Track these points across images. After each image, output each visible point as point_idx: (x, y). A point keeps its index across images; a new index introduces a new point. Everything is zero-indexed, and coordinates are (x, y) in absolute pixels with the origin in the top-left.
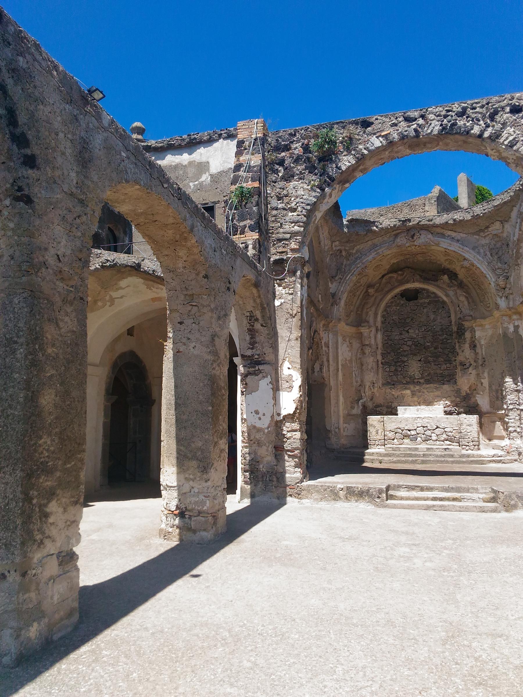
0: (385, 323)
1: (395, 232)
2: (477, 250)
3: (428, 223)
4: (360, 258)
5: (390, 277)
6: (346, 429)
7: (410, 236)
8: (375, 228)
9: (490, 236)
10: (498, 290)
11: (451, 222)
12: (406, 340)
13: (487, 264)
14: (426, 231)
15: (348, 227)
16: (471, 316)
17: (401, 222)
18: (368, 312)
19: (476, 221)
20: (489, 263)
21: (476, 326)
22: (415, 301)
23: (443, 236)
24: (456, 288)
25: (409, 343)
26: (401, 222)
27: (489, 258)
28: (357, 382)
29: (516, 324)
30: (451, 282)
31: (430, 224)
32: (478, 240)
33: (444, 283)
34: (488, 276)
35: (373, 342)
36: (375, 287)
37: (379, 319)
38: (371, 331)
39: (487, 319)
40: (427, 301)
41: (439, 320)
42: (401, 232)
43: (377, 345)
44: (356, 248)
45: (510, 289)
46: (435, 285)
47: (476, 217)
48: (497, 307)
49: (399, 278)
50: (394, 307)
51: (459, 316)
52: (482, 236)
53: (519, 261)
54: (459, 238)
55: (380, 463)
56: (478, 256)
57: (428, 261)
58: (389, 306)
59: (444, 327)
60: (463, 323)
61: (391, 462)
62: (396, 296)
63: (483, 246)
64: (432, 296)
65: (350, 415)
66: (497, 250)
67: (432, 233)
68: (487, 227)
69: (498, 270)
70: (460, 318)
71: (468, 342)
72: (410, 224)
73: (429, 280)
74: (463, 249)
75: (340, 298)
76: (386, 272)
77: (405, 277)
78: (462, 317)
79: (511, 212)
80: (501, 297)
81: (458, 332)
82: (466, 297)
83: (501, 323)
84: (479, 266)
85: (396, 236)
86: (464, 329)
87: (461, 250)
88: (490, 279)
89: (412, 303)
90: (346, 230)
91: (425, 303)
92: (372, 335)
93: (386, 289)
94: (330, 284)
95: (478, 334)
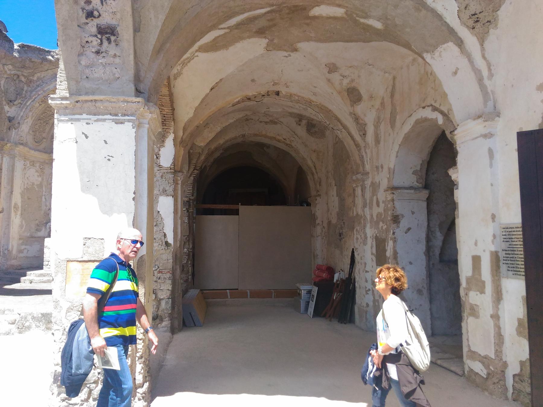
4: (42, 85)
6: (25, 251)
28: (46, 206)
55: (31, 283)
61: (40, 282)
65: (32, 237)
75: (19, 123)
90: (16, 54)
94: (6, 108)
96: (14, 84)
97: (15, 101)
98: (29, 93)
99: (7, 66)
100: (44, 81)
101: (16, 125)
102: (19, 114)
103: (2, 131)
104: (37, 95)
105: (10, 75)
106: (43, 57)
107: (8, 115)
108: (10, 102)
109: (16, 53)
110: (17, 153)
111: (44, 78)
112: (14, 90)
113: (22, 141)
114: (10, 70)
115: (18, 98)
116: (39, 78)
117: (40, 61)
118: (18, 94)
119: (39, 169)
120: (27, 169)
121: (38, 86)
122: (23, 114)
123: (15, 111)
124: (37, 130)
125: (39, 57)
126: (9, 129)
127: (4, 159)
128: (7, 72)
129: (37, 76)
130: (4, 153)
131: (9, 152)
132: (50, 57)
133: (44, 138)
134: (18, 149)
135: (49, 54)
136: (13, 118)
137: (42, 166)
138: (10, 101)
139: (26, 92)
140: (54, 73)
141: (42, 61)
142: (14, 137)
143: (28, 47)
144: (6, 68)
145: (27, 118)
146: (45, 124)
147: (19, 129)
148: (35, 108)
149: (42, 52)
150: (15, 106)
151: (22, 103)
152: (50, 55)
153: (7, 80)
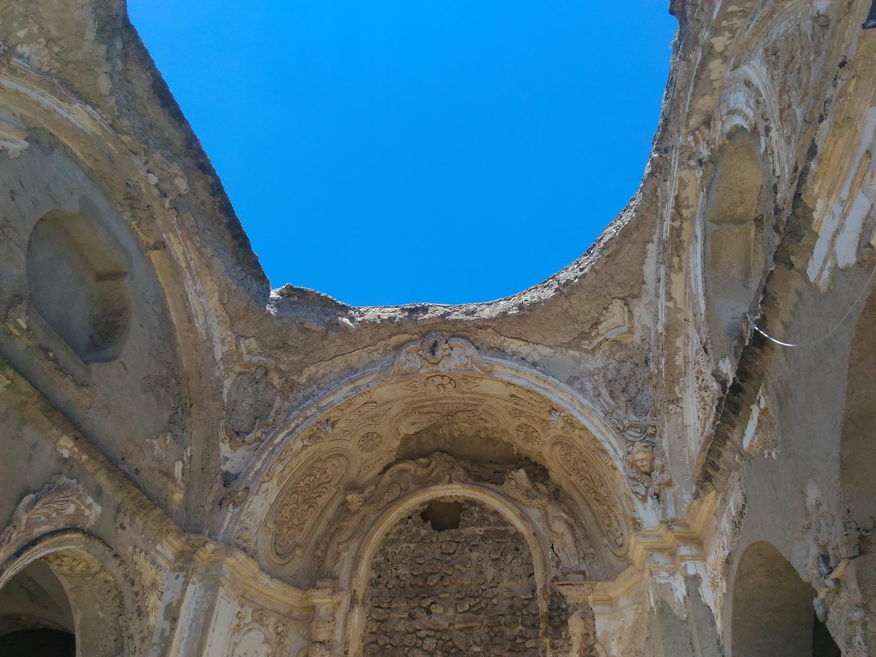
0: (377, 584)
1: (394, 340)
2: (577, 385)
3: (465, 318)
5: (402, 471)
7: (428, 349)
8: (346, 320)
9: (605, 347)
10: (634, 479)
11: (514, 311)
12: (422, 634)
13: (603, 415)
14: (463, 340)
15: (278, 304)
16: (583, 573)
17: (406, 314)
18: (339, 553)
19: (567, 304)
20: (606, 414)
21: (596, 602)
22: (453, 531)
23: (501, 352)
24: (545, 501)
25: (430, 644)
26: (406, 314)
27: (608, 404)
29: (691, 571)
30: (534, 486)
31: (468, 321)
32: (579, 362)
33: (517, 486)
34: (607, 446)
35: (338, 636)
36: (366, 492)
37: (363, 568)
38: (339, 604)
39: (621, 579)
40: (479, 531)
41: (506, 583)
42: (409, 341)
43: (346, 643)
44: (306, 373)
45: (662, 472)
46: (497, 492)
47: (566, 290)
48: (636, 524)
49: (420, 472)
50: (404, 545)
51: (554, 572)
52: (586, 351)
53: (677, 389)
54: (537, 359)
56: (580, 397)
57: (483, 434)
58: (393, 541)
59: (518, 603)
60: (563, 590)
62: (410, 518)
63: (591, 374)
64: (492, 519)
66: (623, 382)
67: (478, 348)
68: (596, 323)
69: (630, 432)
70: (556, 578)
71: (576, 647)
72: (426, 316)
73: (485, 481)
74: (545, 381)
76: (394, 459)
77: (432, 471)
78: (560, 576)
79: (643, 263)
80: (644, 499)
81: (550, 618)
82: (570, 526)
83: (651, 573)
84: (584, 421)
85: (398, 348)
86: (566, 610)
87: (542, 384)
88: (611, 452)
89: (444, 536)
90: (272, 310)
91: (475, 536)
92: (340, 616)
93: (388, 498)
94: (225, 449)
95: (601, 625)
96: (253, 393)
97: (248, 434)
98: (283, 416)
99: (247, 341)
100: (322, 386)
101: (239, 494)
102: (252, 467)
103: (202, 506)
104: (301, 419)
105: (250, 364)
106: (330, 321)
107: (224, 468)
108: (237, 435)
109: (272, 308)
110: (228, 576)
111: (324, 379)
112: (251, 405)
113: (245, 541)
114: (250, 352)
115: (257, 425)
116: (312, 378)
117: (321, 328)
118: (259, 416)
119: (274, 636)
120: (242, 632)
121: (306, 398)
122: (261, 468)
123: (244, 458)
124: (285, 519)
125: (321, 319)
126: (220, 504)
127: (190, 588)
128: (243, 358)
129: (308, 373)
130: (193, 569)
131: (207, 571)
132: (346, 320)
133: (297, 545)
134: (231, 561)
135: (344, 314)
136: (236, 476)
137: (284, 625)
138: (238, 433)
139: (278, 413)
140: (349, 365)
141: (328, 330)
142: (227, 529)
143: (302, 293)
144: (243, 345)
145: (269, 479)
146: (305, 507)
147: (243, 506)
148: (291, 453)
149: (330, 310)
150: (245, 446)
151: (263, 438)
152: (346, 316)
153: (239, 379)
